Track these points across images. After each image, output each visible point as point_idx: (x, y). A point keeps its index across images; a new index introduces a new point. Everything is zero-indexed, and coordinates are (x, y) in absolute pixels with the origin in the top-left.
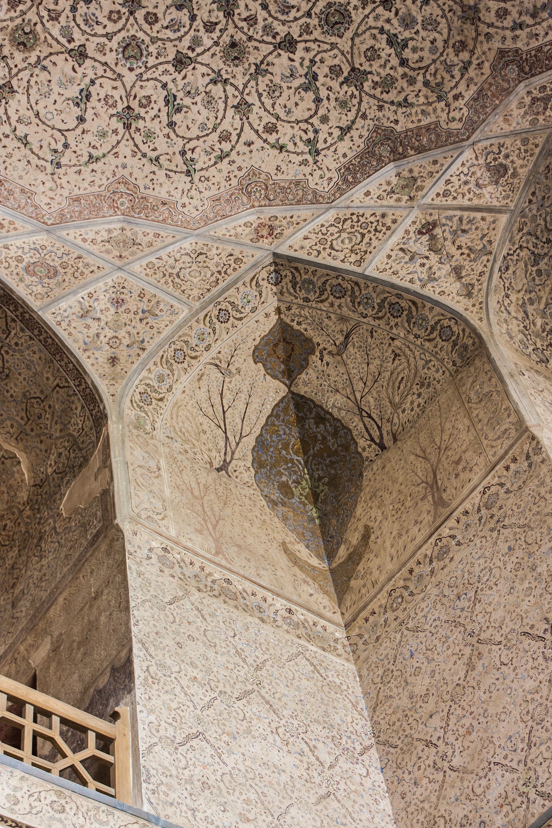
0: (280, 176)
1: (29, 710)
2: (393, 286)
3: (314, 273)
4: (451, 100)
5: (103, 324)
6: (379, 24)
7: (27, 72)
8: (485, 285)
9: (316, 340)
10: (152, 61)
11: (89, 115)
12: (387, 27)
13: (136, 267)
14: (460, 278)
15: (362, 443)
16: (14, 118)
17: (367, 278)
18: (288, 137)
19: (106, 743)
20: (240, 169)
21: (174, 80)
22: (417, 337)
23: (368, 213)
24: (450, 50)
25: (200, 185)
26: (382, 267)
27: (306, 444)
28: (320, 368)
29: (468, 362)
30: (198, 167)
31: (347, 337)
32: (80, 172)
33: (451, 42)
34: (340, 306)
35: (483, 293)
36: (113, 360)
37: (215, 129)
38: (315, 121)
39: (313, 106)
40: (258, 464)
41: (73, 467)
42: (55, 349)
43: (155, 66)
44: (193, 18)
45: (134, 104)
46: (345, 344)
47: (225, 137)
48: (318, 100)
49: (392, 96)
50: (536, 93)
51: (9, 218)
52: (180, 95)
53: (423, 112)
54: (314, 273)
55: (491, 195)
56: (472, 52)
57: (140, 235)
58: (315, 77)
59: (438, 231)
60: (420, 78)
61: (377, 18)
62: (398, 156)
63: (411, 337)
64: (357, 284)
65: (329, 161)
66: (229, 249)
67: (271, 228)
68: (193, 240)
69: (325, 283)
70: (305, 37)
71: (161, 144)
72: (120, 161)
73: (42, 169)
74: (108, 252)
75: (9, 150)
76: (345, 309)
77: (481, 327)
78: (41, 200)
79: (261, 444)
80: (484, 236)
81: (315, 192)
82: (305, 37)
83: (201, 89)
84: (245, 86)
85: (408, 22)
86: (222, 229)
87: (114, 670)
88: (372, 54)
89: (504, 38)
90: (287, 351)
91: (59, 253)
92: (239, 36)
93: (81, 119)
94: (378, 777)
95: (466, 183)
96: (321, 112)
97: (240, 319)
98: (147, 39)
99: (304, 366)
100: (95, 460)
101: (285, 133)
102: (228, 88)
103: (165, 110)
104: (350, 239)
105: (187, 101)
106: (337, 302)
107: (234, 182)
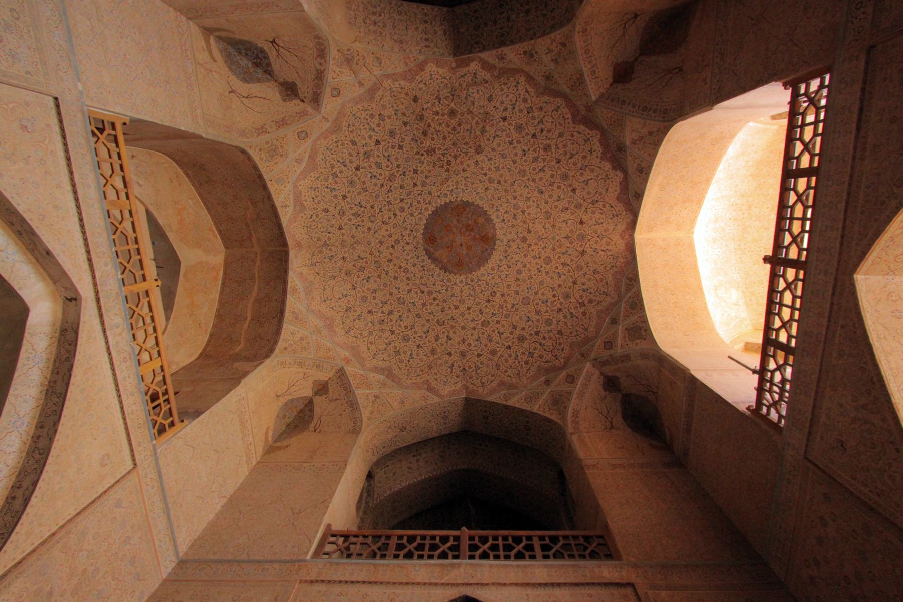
1: (166, 397)
13: (314, 337)
15: (312, 425)
19: (172, 424)
27: (301, 411)
29: (353, 433)
36: (286, 348)
40: (286, 404)
41: (248, 359)
42: (278, 332)
55: (396, 405)
62: (388, 377)
65: (374, 362)
71: (348, 321)
77: (363, 428)
79: (292, 400)
87: (196, 411)
88: (405, 352)
90: (322, 389)
94: (219, 507)
100: (255, 363)
101: (372, 347)
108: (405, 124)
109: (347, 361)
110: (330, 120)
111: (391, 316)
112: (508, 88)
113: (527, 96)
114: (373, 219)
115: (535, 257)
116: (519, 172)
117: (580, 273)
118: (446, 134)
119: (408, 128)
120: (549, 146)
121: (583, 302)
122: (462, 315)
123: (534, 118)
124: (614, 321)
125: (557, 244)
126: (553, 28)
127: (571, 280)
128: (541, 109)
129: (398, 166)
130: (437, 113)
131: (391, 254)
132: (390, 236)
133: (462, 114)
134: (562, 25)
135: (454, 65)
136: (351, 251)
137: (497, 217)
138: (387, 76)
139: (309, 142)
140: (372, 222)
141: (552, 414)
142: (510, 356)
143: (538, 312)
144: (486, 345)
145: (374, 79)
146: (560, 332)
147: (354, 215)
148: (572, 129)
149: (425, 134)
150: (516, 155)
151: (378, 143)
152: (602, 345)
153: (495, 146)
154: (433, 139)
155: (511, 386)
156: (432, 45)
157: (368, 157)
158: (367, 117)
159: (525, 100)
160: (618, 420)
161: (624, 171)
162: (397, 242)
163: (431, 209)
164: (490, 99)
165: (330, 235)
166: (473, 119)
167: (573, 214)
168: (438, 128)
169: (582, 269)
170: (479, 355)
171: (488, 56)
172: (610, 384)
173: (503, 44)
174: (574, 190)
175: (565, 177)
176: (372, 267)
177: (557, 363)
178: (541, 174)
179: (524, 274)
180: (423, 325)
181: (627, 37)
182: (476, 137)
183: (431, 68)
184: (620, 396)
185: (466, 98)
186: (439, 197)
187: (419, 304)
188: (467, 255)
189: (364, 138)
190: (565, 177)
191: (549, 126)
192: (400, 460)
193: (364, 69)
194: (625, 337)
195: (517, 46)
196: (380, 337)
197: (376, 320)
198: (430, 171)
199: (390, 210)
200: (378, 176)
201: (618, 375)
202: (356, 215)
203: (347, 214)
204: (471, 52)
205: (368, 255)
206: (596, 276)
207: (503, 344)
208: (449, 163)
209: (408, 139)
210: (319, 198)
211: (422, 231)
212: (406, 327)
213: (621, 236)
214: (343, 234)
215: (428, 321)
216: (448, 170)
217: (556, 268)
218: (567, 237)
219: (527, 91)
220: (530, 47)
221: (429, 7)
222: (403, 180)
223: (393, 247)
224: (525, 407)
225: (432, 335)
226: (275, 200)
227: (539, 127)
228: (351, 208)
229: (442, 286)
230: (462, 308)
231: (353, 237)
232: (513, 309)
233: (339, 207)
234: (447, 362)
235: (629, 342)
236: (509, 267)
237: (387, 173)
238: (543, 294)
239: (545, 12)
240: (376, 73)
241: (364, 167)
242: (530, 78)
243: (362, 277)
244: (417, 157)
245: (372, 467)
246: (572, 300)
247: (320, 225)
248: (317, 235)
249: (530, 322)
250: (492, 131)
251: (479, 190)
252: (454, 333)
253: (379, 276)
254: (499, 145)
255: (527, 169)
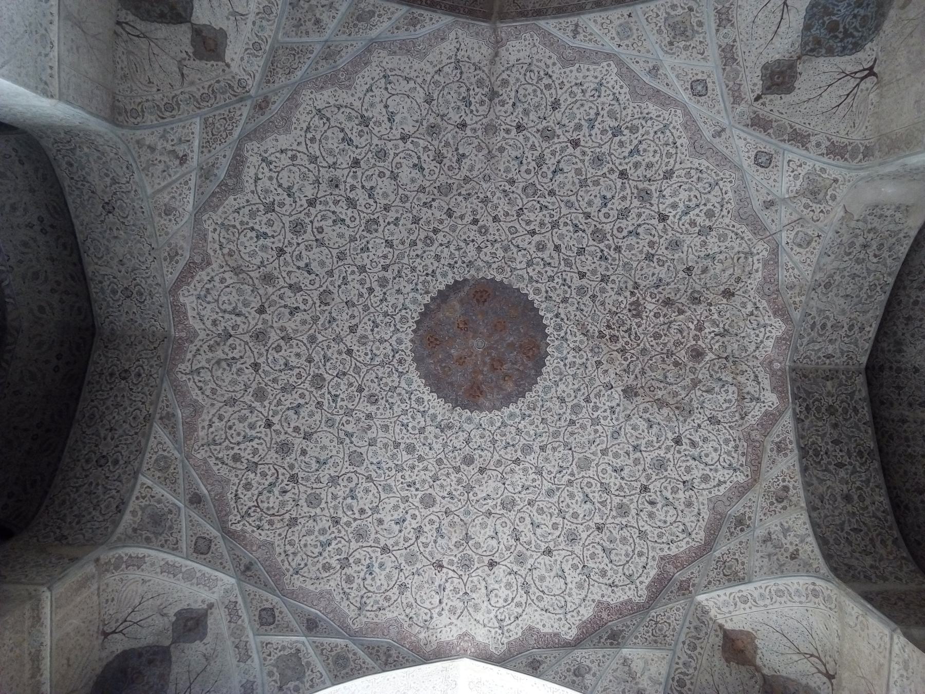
0: (273, 137)
2: (180, 120)
3: (225, 100)
4: (217, 227)
5: (319, 5)
6: (276, 238)
7: (424, 115)
8: (134, 153)
9: (197, 61)
10: (370, 155)
11: (384, 110)
12: (272, 240)
13: (318, 48)
14: (149, 147)
16: (418, 88)
17: (197, 115)
18: (282, 159)
20: (295, 129)
21: (354, 152)
22: (147, 100)
23: (218, 147)
24: (234, 249)
25: (309, 108)
26: (193, 126)
28: (183, 47)
30: (317, 117)
31: (182, 75)
32: (373, 79)
33: (237, 252)
34: (199, 90)
35: (131, 148)
37: (320, 141)
38: (275, 175)
39: (281, 181)
43: (366, 154)
44: (363, 187)
45: (365, 129)
46: (181, 70)
47: (313, 140)
48: (280, 186)
49: (246, 211)
50: (178, 258)
51: (395, 34)
52: (347, 147)
53: (226, 212)
54: (225, 100)
55: (165, 198)
56: (223, 255)
57: (324, 64)
58: (289, 195)
59: (177, 162)
60: (239, 227)
61: (280, 240)
63: (150, 98)
64: (199, 108)
66: (276, 85)
67: (261, 108)
68: (297, 78)
69: (216, 98)
70: (306, 211)
71: (342, 118)
72: (356, 97)
73: (392, 70)
74: (336, 46)
75: (413, 70)
76: (195, 90)
78: (384, 53)
80: (153, 175)
81: (251, 140)
82: (306, 211)
83: (338, 156)
84: (319, 170)
85: (264, 248)
86: (286, 94)
88: (270, 223)
89: (213, 271)
91: (361, 31)
92: (337, 191)
93: (386, 107)
95: (180, 195)
96: (275, 181)
97: (246, 50)
98: (378, 164)
99: (193, 41)
101: (285, 160)
102: (326, 165)
103: (350, 135)
104: (218, 128)
105: (342, 146)
106: (202, 91)
107: (294, 120)
108: (689, 270)
109: (262, 106)
110: (718, 139)
111: (343, 204)
112: (728, 453)
113: (713, 483)
114: (530, 191)
115: (435, 478)
116: (586, 458)
117: (401, 560)
118: (664, 339)
119: (681, 275)
120: (626, 514)
121: (349, 566)
122: (338, 339)
123: (675, 491)
124: (312, 625)
125: (456, 519)
126: (822, 541)
127: (390, 543)
128: (689, 504)
129: (618, 249)
130: (700, 328)
131: (462, 217)
132: (496, 219)
133: (693, 370)
134: (828, 557)
135: (777, 366)
136: (476, 142)
137: (512, 415)
138: (775, 252)
139: (685, 96)
140: (524, 189)
141: (134, 513)
142: (252, 427)
143: (334, 481)
144: (275, 380)
145: (774, 228)
146: (293, 522)
147: (542, 156)
148: (651, 554)
149: (668, 302)
150: (616, 455)
151: (663, 218)
152: (267, 605)
153: (635, 420)
154: (657, 315)
155: (191, 428)
156: (814, 334)
157: (641, 198)
158: (709, 206)
159: (705, 479)
160: (119, 645)
161: (577, 643)
162: (483, 231)
163: (537, 300)
164: (713, 420)
165: (508, 107)
166: (684, 388)
167: (508, 549)
168: (674, 326)
169: (410, 563)
170: (256, 366)
171: (786, 426)
172: (192, 624)
173: (804, 452)
174: (548, 552)
175: (572, 538)
176: (443, 179)
177: (234, 517)
178: (579, 497)
179: (406, 457)
180: (322, 264)
181: (796, 657)
182: (652, 389)
183: (778, 328)
184: (167, 643)
185: (720, 380)
186: (557, 316)
187: (364, 259)
188: (450, 356)
189: (674, 194)
190: (572, 538)
191: (660, 515)
192: (32, 191)
193: (795, 217)
194: (284, 648)
195: (798, 477)
196: (304, 177)
197: (338, 173)
198: (603, 304)
199: (542, 224)
200: (604, 210)
201: (209, 639)
202: (540, 161)
203: (545, 145)
204: (796, 397)
205: (464, 172)
206: (395, 590)
207: (275, 413)
208: (614, 339)
209: (662, 272)
210: (579, 96)
211: (498, 278)
212: (321, 230)
213: (465, 634)
214: (508, 131)
215: (330, 273)
216: (601, 335)
217: (414, 517)
218: (467, 538)
219: (720, 483)
220: (794, 499)
221: (872, 335)
222: (592, 255)
223: (475, 222)
224: (149, 458)
225: (303, 278)
226: (592, 15)
227: (659, 499)
228: (553, 153)
229: (394, 306)
230: (350, 341)
231: (501, 150)
232: (342, 435)
233: (559, 132)
234: (246, 304)
235: (274, 658)
236: (422, 430)
237: (608, 228)
238: (367, 491)
239: (847, 528)
240: (784, 234)
241: (623, 188)
242: (742, 490)
243: (424, 157)
244: (630, 284)
245: (24, 132)
246: (354, 545)
247: (530, 89)
248: (512, 81)
249: (314, 466)
250: (659, 418)
251: (562, 386)
252: (304, 322)
253: (422, 189)
254: (635, 428)
255: (590, 473)
